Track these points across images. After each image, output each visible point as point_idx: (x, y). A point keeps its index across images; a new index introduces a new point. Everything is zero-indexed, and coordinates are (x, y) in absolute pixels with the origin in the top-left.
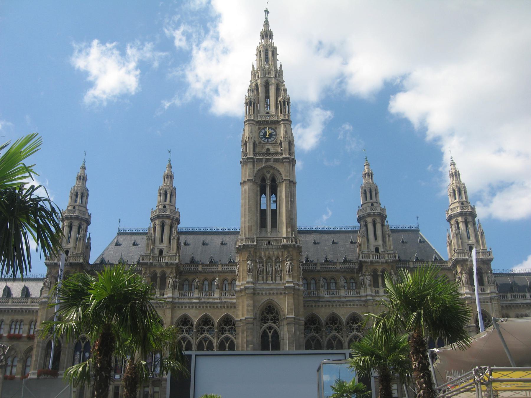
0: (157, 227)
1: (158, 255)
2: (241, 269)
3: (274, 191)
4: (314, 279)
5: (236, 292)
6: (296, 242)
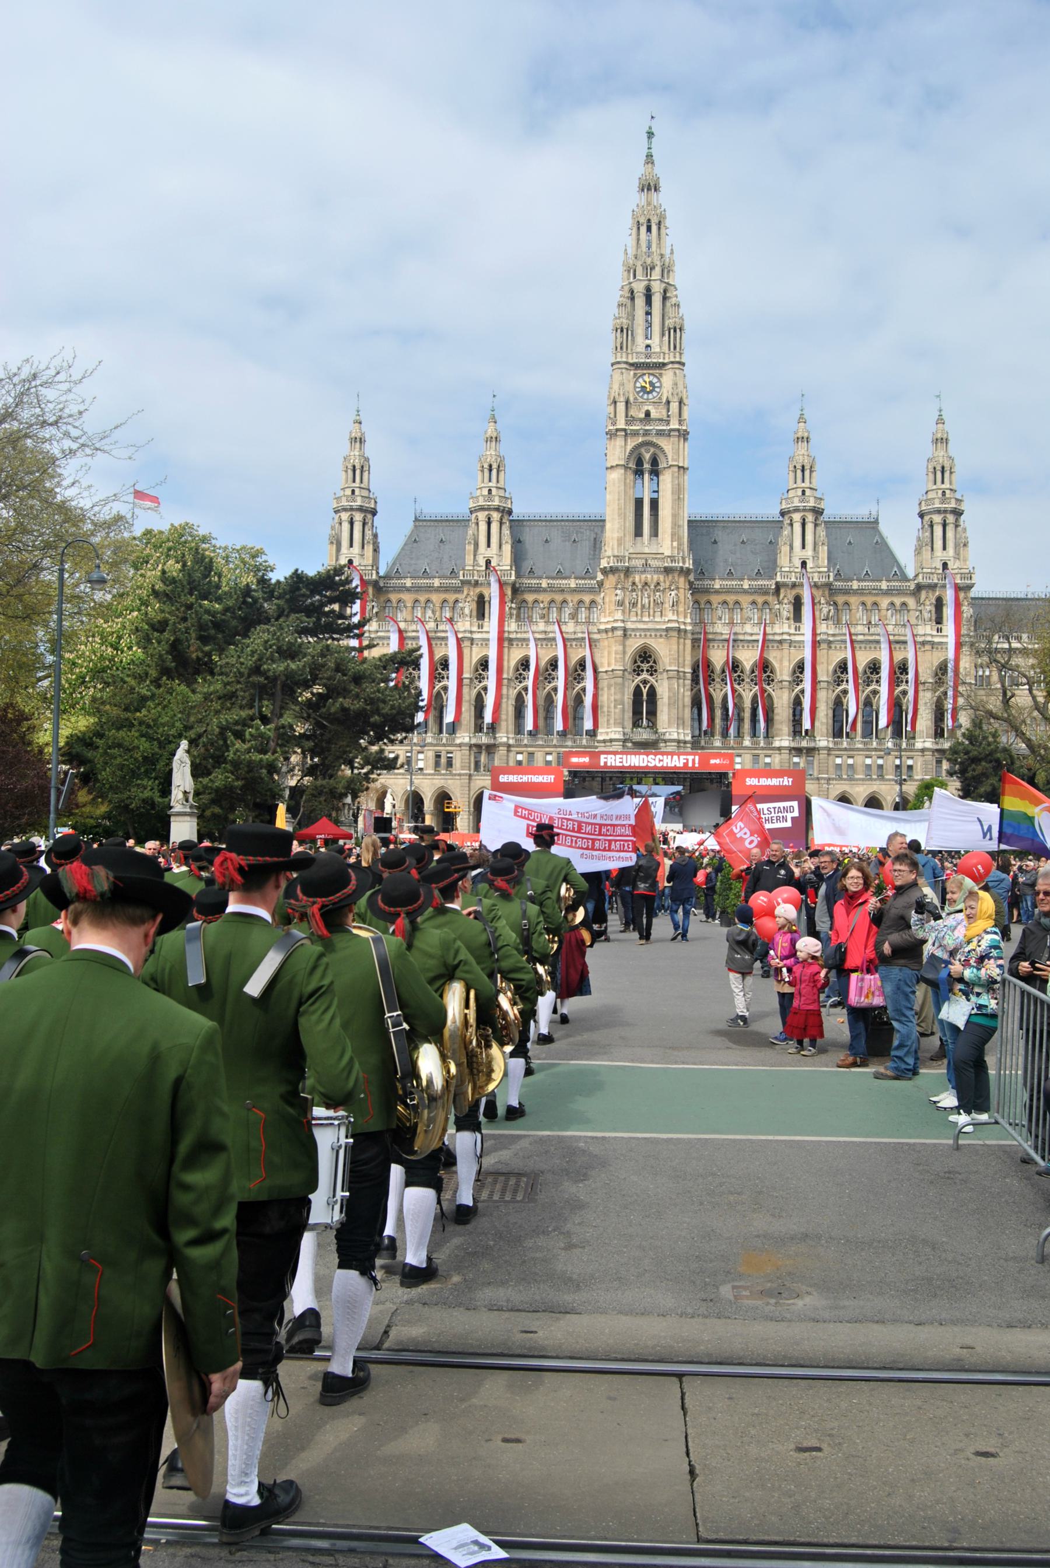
0: (480, 523)
1: (484, 568)
2: (607, 600)
3: (655, 472)
5: (599, 631)
6: (684, 563)
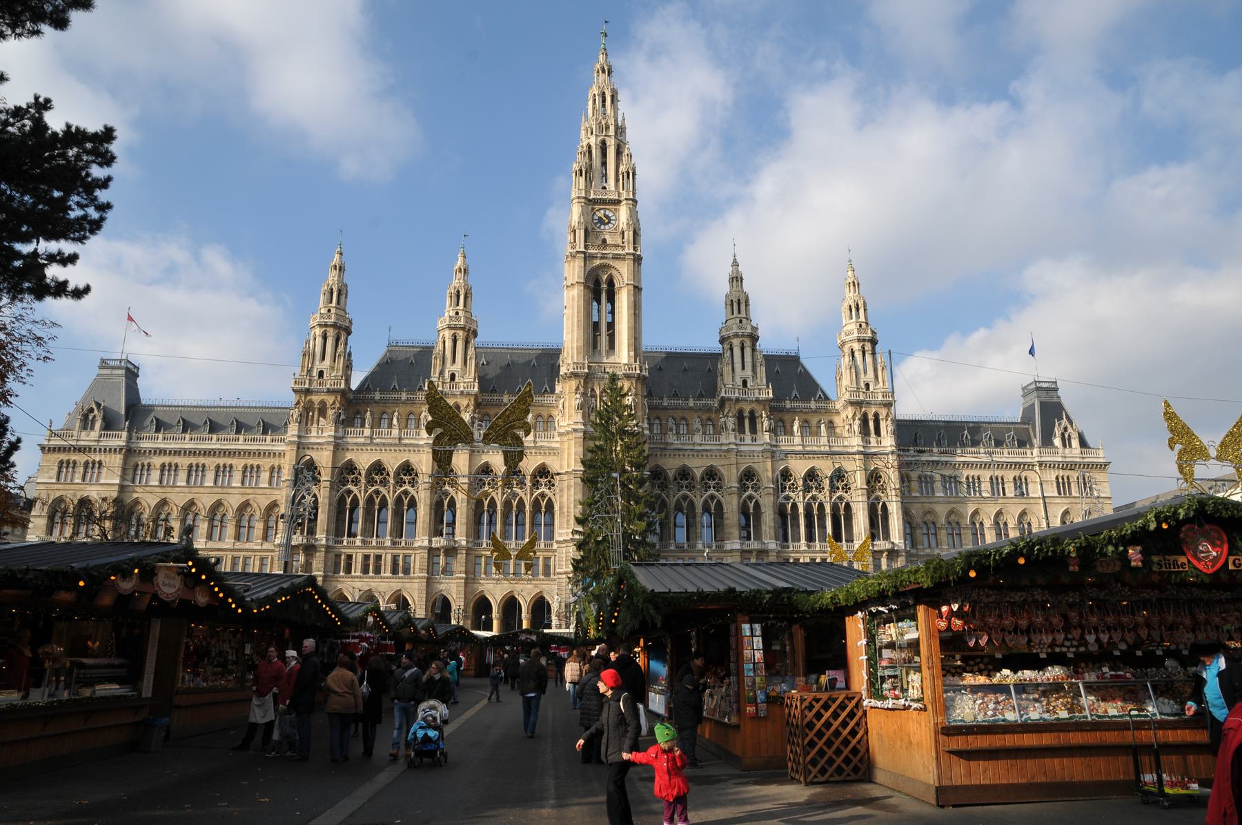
2: (567, 405)
3: (611, 299)
4: (658, 418)
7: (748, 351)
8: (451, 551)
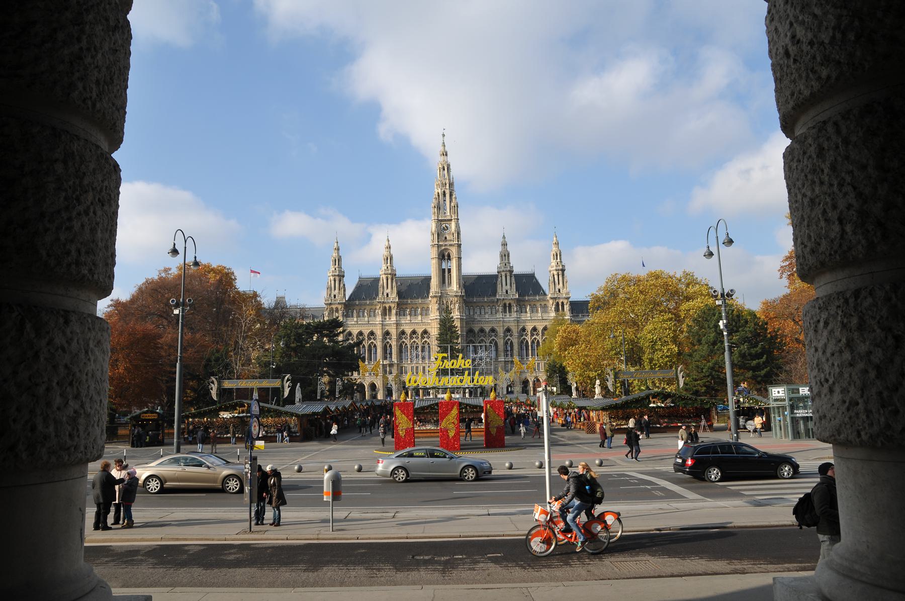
3: (449, 258)
7: (508, 277)
8: (391, 365)
